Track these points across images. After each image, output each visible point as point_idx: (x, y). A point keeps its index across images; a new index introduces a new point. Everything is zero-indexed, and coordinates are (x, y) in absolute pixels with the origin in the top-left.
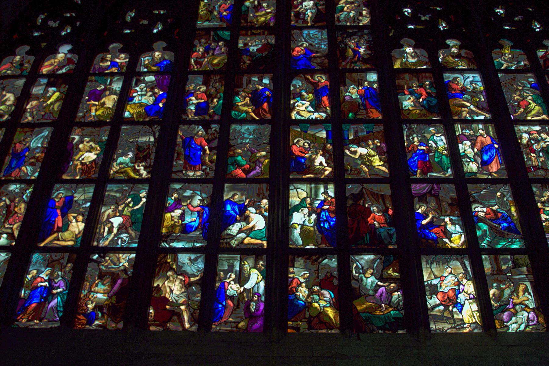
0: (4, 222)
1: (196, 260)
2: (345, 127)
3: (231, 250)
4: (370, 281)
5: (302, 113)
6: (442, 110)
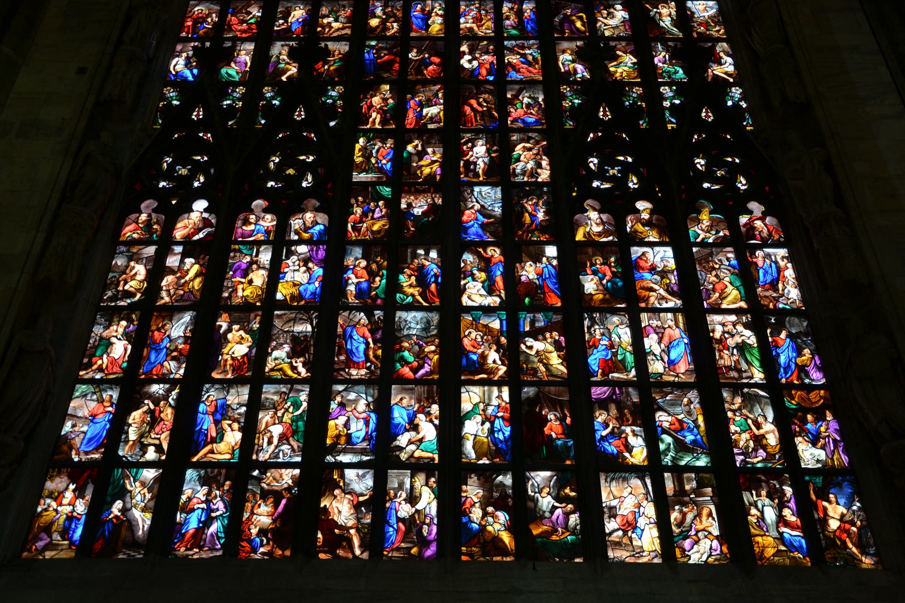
0: (149, 432)
1: (364, 476)
2: (522, 315)
3: (402, 465)
4: (546, 502)
5: (473, 297)
6: (627, 298)
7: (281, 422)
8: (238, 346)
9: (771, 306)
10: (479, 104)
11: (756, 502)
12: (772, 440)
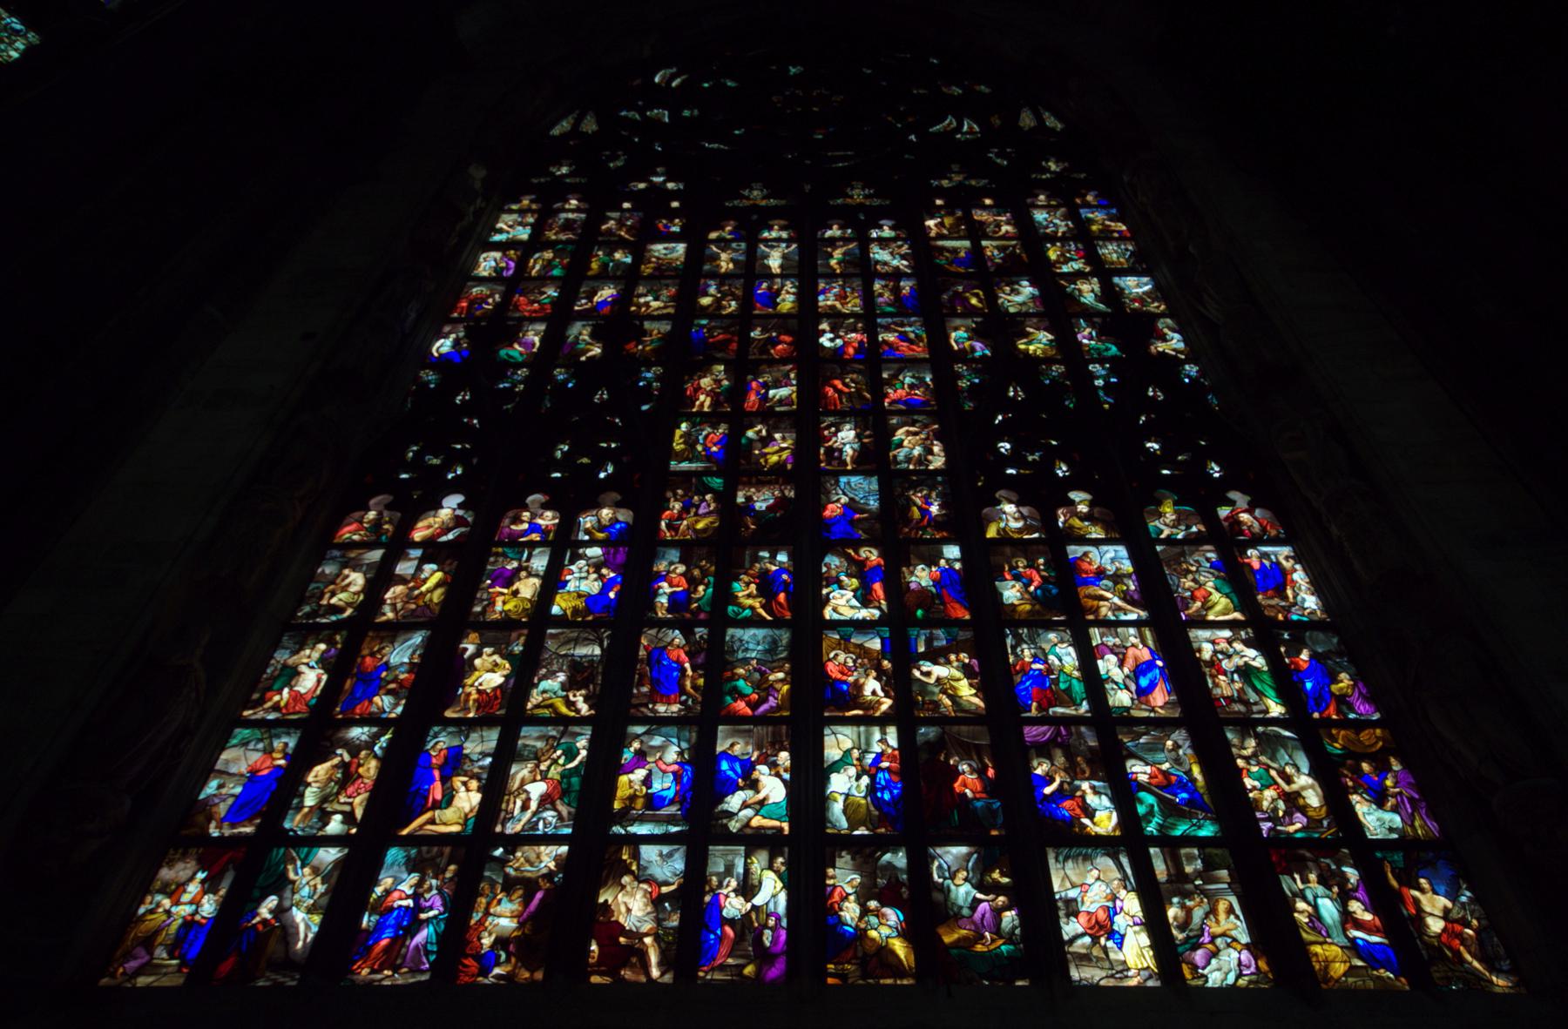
1: (670, 855)
2: (913, 632)
4: (962, 892)
5: (841, 610)
6: (1066, 604)
7: (544, 779)
8: (489, 675)
9: (1280, 617)
10: (845, 385)
11: (1302, 891)
12: (1313, 799)
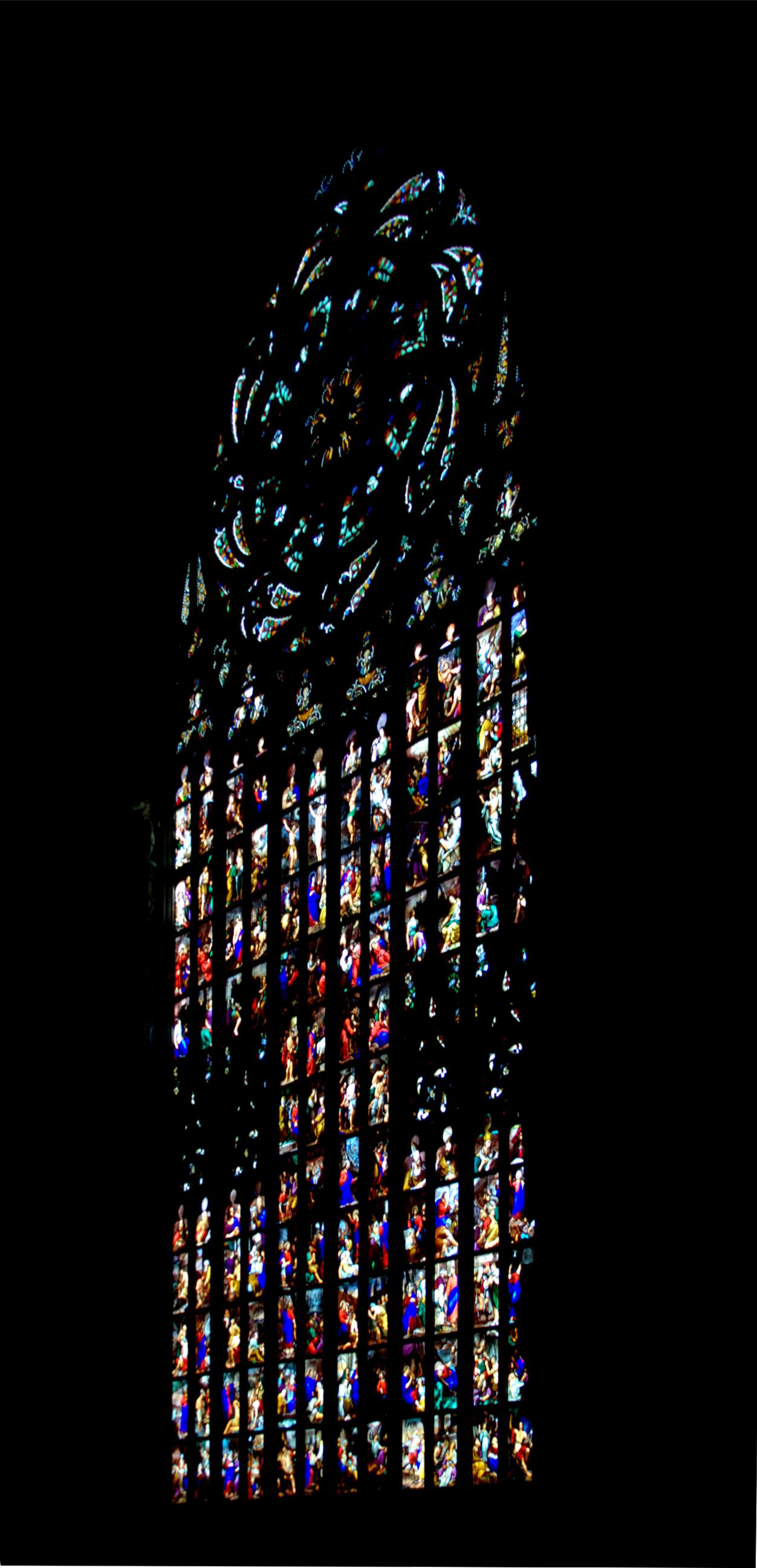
4: (376, 1445)
12: (496, 1380)
